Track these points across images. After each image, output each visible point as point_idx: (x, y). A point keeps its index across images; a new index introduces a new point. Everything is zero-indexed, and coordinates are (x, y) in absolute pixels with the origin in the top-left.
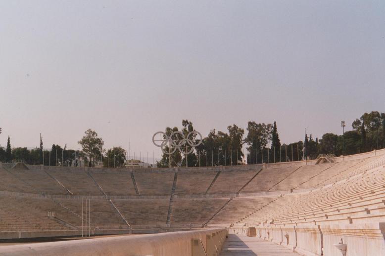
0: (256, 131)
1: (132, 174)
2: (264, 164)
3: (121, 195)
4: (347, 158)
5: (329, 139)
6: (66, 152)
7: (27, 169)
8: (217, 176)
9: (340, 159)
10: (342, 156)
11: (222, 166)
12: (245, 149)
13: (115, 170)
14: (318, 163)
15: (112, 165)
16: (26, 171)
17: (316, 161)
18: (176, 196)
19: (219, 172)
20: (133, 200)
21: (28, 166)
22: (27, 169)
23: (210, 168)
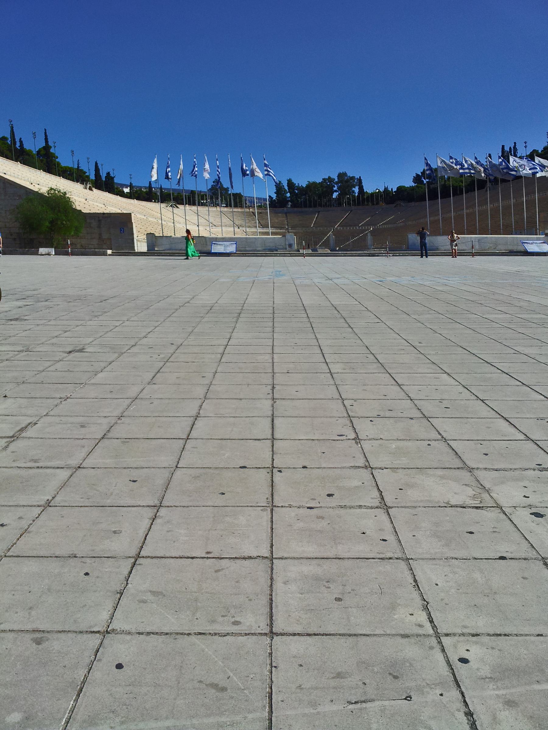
2: (353, 206)
4: (417, 204)
5: (400, 189)
7: (177, 207)
9: (413, 204)
10: (413, 202)
11: (320, 207)
12: (335, 195)
14: (395, 207)
16: (178, 209)
17: (394, 205)
18: (290, 228)
19: (319, 212)
21: (178, 205)
22: (177, 207)
23: (311, 209)
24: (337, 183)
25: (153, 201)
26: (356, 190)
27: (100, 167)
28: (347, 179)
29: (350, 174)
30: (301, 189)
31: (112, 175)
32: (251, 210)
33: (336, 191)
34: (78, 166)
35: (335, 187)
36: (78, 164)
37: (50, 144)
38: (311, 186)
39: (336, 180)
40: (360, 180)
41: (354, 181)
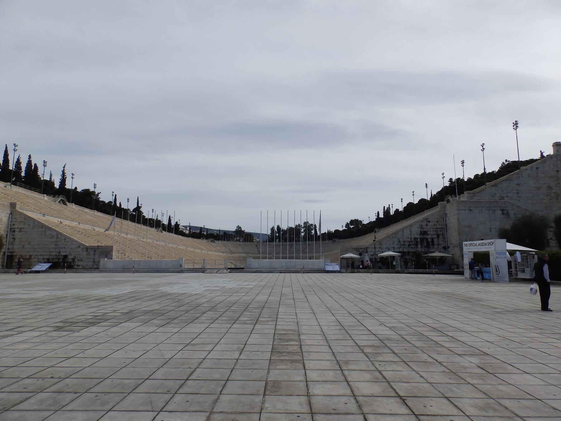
0: (308, 227)
1: (256, 245)
3: (252, 253)
6: (229, 235)
8: (291, 246)
13: (249, 243)
15: (248, 241)
16: (215, 243)
20: (258, 256)
21: (215, 241)
24: (303, 228)
25: (202, 238)
26: (313, 232)
27: (171, 217)
28: (309, 225)
29: (310, 223)
30: (285, 232)
31: (178, 223)
32: (256, 243)
33: (302, 232)
34: (157, 218)
35: (302, 230)
36: (157, 217)
37: (140, 205)
38: (291, 229)
39: (303, 226)
40: (315, 226)
41: (312, 227)
